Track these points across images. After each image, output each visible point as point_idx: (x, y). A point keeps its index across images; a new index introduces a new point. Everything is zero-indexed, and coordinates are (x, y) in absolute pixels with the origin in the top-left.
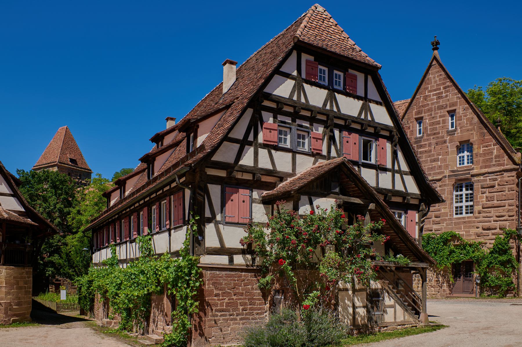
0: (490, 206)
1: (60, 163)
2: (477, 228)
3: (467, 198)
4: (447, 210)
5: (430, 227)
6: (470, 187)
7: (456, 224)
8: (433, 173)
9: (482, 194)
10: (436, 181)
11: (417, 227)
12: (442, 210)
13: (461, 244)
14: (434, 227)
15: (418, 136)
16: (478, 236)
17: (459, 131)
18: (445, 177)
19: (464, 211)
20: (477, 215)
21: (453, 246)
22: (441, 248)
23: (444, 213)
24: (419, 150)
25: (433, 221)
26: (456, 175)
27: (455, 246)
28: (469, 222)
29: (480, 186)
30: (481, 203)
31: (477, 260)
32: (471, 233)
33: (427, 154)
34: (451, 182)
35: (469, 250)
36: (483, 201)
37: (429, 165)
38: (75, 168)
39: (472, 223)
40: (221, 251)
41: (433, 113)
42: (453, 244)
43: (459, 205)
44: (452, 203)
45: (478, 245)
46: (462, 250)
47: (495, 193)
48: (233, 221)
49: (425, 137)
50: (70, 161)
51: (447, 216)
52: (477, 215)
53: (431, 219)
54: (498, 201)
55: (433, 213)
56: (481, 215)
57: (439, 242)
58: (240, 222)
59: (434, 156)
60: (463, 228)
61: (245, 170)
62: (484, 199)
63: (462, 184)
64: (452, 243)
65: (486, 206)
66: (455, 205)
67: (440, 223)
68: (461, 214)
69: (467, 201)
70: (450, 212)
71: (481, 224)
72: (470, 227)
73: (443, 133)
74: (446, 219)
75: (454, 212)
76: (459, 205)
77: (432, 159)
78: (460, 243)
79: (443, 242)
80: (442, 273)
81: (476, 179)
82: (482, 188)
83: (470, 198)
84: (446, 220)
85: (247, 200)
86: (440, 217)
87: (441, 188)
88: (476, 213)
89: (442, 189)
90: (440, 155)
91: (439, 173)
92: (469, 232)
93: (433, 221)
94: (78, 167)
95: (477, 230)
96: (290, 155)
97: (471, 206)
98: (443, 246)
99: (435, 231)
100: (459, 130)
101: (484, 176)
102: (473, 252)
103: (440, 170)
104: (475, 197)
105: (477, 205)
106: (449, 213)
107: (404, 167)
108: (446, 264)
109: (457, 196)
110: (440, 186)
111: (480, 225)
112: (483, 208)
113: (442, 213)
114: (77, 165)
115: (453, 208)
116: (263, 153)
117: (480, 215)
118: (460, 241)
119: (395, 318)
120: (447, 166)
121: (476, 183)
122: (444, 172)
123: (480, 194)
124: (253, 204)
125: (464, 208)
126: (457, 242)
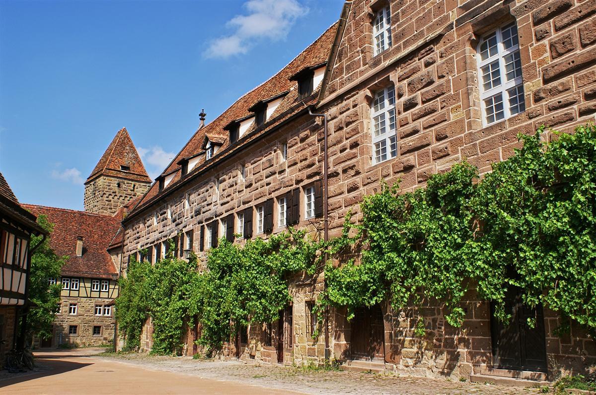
0: (564, 69)
8: (428, 29)
9: (538, 40)
10: (432, 46)
18: (450, 27)
34: (462, 34)
36: (543, 60)
47: (576, 26)
53: (430, 147)
54: (584, 46)
55: (433, 128)
56: (544, 103)
62: (548, 54)
65: (552, 74)
74: (460, 139)
82: (536, 24)
86: (446, 137)
87: (444, 60)
88: (530, 102)
91: (438, 24)
112: (546, 82)
113: (450, 124)
121: (521, 13)
123: (534, 42)
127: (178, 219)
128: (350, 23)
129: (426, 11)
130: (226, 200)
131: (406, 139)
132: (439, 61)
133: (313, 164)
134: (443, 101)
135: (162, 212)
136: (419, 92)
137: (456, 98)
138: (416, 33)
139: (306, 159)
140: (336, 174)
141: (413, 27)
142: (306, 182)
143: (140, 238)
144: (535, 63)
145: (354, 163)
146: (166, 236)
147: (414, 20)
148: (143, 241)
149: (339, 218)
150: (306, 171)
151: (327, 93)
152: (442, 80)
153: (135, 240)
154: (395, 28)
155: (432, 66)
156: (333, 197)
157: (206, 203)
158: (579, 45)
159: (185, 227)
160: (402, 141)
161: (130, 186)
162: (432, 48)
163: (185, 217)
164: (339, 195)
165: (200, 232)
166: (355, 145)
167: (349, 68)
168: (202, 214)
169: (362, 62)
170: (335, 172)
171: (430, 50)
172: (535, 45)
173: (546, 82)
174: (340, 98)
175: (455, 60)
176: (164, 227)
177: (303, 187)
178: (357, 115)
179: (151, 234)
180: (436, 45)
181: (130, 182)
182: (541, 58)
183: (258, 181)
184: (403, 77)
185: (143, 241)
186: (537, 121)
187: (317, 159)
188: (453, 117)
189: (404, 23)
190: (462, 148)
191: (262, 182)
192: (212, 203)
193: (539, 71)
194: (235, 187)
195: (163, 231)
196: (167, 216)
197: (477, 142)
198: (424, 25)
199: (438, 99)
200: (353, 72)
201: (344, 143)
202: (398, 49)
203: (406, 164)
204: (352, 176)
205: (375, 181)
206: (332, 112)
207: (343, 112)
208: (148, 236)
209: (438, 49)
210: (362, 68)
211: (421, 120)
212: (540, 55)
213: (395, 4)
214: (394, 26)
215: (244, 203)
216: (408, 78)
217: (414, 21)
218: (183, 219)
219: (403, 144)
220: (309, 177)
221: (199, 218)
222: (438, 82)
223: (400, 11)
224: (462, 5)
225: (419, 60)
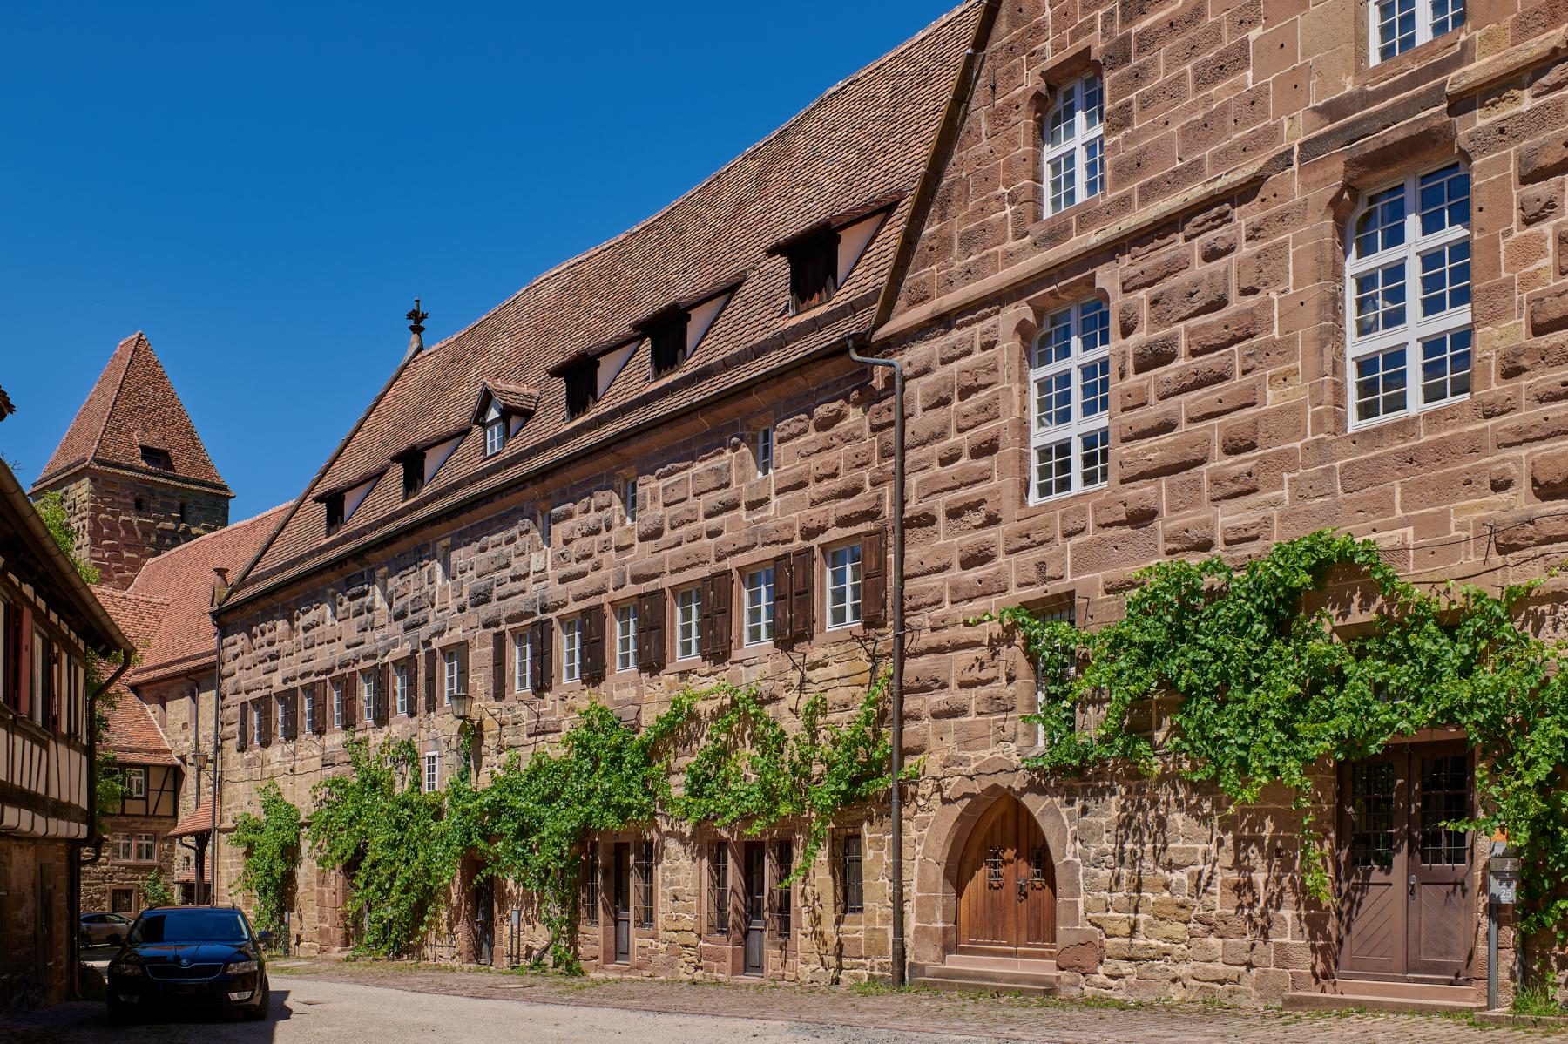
1: (100, 462)
2: (1499, 486)
4: (1298, 391)
5: (1198, 525)
8: (1215, 157)
9: (1528, 222)
10: (1227, 206)
12: (1269, 393)
13: (1389, 615)
14: (1221, 519)
16: (1500, 552)
18: (1284, 159)
20: (1494, 387)
21: (1336, 638)
22: (1256, 655)
23: (1280, 411)
24: (1136, 28)
26: (1349, 135)
27: (1347, 634)
28: (1444, 452)
29: (1512, 167)
31: (1492, 730)
32: (1454, 534)
33: (1178, 41)
34: (1316, 184)
35: (1434, 659)
36: (1534, 275)
37: (1191, 110)
38: (163, 480)
39: (1458, 457)
42: (1340, 623)
44: (1334, 334)
45: (1499, 611)
46: (1395, 658)
50: (143, 458)
51: (1298, 432)
52: (1496, 388)
53: (1203, 468)
55: (1215, 421)
56: (1523, 382)
57: (1238, 617)
59: (1219, 40)
60: (1398, 498)
63: (1400, 188)
64: (1328, 620)
66: (1356, 347)
67: (1254, 490)
69: (1432, 306)
71: (1522, 452)
72: (1444, 490)
74: (1290, 455)
75: (1352, 399)
77: (1205, 64)
78: (1379, 611)
79: (1267, 612)
80: (1267, 833)
81: (1482, 119)
82: (1525, 180)
84: (1287, 460)
86: (1252, 446)
87: (1258, 247)
88: (1488, 377)
89: (1266, 250)
90: (1252, 23)
91: (1245, 149)
92: (1442, 520)
93: (1215, 482)
94: (175, 478)
95: (1492, 506)
97: (1463, 337)
98: (1266, 642)
99: (1228, 543)
101: (1544, 80)
102: (1465, 671)
103: (1256, 122)
104: (1477, 260)
105: (1494, 317)
106: (1310, 410)
108: (1274, 770)
109: (1365, 282)
111: (1517, 461)
112: (1538, 330)
113: (1267, 414)
114: (172, 468)
115: (1337, 368)
117: (1518, 390)
118: (1380, 600)
120: (1295, 85)
122: (1277, 128)
123: (1514, 226)
126: (1363, 607)
127: (413, 612)
128: (979, 114)
129: (1214, 106)
130: (575, 567)
131: (1136, 443)
132: (1245, 250)
133: (856, 490)
134: (1248, 355)
135: (354, 591)
136: (1181, 325)
137: (1284, 348)
138: (1178, 164)
139: (834, 475)
140: (927, 520)
141: (1172, 149)
142: (834, 534)
143: (278, 658)
144: (1512, 280)
145: (982, 494)
146: (374, 656)
147: (1174, 129)
148: (287, 667)
149: (933, 630)
150: (833, 506)
151: (901, 303)
152: (1251, 300)
153: (261, 662)
154: (1116, 143)
155: (1224, 259)
156: (916, 576)
157: (507, 572)
159: (440, 633)
162: (1227, 213)
163: (437, 607)
164: (935, 572)
165: (491, 648)
166: (986, 449)
167: (968, 241)
168: (495, 603)
169: (1010, 229)
170: (925, 515)
171: (1220, 216)
172: (1516, 234)
173: (1538, 330)
174: (943, 321)
175: (1291, 251)
176: (365, 630)
177: (823, 547)
178: (995, 370)
179: (317, 648)
180: (1239, 205)
182: (1531, 269)
183: (682, 524)
184: (1136, 282)
185: (287, 667)
186: (1502, 423)
187: (868, 478)
188: (1272, 398)
189: (1145, 132)
190: (1292, 475)
191: (694, 526)
192: (527, 575)
193: (1521, 302)
194: (604, 536)
195: (363, 643)
196: (373, 601)
197: (1337, 464)
198: (1205, 146)
199: (1235, 348)
200: (984, 253)
201: (951, 440)
202: (1123, 204)
203: (1132, 506)
204: (976, 527)
205: (1041, 543)
206: (918, 355)
207: (951, 360)
208: (306, 654)
209: (1244, 217)
210: (1011, 245)
211: (1184, 398)
212: (1527, 262)
213: (1122, 76)
214: (1115, 139)
215: (637, 579)
216: (1150, 284)
217: (1175, 129)
218: (431, 614)
219: (1128, 455)
220: (844, 522)
221: (486, 611)
222: (1237, 304)
223: (1133, 96)
224: (1319, 104)
225: (1187, 239)
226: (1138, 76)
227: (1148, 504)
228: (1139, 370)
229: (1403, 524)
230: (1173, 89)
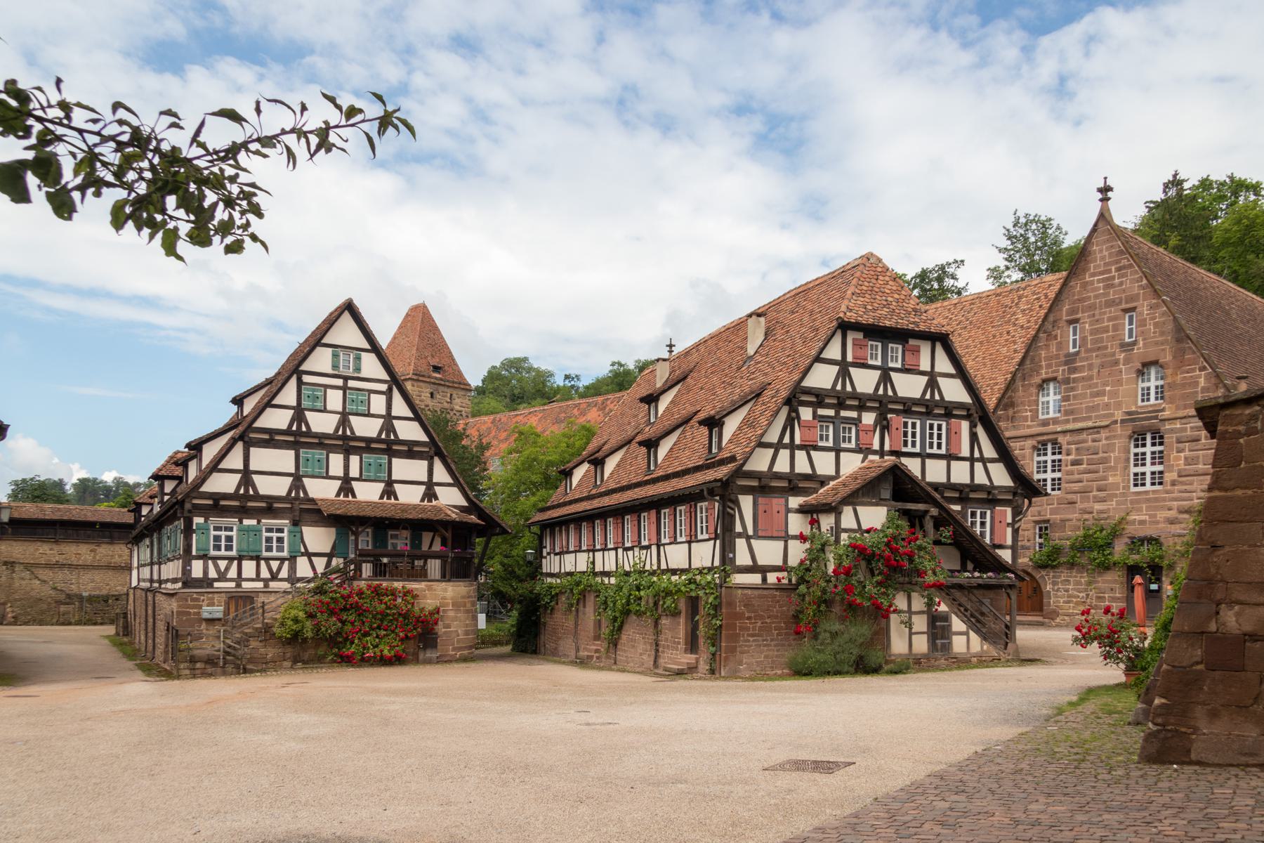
2: (1170, 509)
3: (1153, 458)
4: (1118, 479)
6: (1158, 438)
7: (1132, 502)
9: (1178, 452)
11: (1009, 530)
12: (1110, 479)
15: (1072, 350)
17: (1141, 345)
18: (1116, 422)
19: (1148, 481)
24: (1072, 376)
25: (1095, 497)
28: (1156, 500)
29: (1174, 439)
30: (1176, 468)
40: (754, 568)
41: (1097, 312)
43: (1140, 469)
44: (1127, 467)
48: (767, 535)
49: (1083, 355)
54: (1205, 465)
58: (774, 535)
61: (779, 476)
65: (1184, 474)
66: (1134, 470)
68: (1143, 485)
69: (1153, 464)
70: (1123, 482)
71: (1175, 503)
72: (1157, 508)
73: (1112, 347)
74: (1116, 494)
75: (1132, 482)
76: (1140, 469)
83: (1159, 458)
84: (1116, 495)
85: (783, 510)
86: (1105, 490)
90: (1108, 385)
92: (1155, 516)
96: (833, 454)
97: (1161, 473)
100: (1141, 343)
107: (989, 451)
110: (1107, 438)
112: (1180, 476)
115: (1129, 475)
116: (801, 456)
119: (968, 647)
124: (789, 515)
125: (1148, 477)
137: (1114, 468)
152: (1105, 455)
158: (1201, 463)
160: (1067, 485)
161: (446, 396)
173: (1180, 476)
181: (446, 390)
188: (1111, 480)
202: (1067, 421)
209: (1104, 434)
210: (1029, 423)
226: (1073, 389)
227: (1075, 500)
228: (1072, 465)
229: (1146, 515)
230: (1084, 396)
